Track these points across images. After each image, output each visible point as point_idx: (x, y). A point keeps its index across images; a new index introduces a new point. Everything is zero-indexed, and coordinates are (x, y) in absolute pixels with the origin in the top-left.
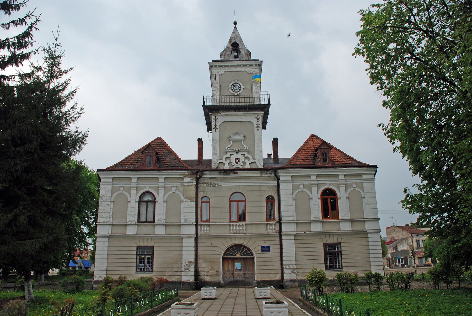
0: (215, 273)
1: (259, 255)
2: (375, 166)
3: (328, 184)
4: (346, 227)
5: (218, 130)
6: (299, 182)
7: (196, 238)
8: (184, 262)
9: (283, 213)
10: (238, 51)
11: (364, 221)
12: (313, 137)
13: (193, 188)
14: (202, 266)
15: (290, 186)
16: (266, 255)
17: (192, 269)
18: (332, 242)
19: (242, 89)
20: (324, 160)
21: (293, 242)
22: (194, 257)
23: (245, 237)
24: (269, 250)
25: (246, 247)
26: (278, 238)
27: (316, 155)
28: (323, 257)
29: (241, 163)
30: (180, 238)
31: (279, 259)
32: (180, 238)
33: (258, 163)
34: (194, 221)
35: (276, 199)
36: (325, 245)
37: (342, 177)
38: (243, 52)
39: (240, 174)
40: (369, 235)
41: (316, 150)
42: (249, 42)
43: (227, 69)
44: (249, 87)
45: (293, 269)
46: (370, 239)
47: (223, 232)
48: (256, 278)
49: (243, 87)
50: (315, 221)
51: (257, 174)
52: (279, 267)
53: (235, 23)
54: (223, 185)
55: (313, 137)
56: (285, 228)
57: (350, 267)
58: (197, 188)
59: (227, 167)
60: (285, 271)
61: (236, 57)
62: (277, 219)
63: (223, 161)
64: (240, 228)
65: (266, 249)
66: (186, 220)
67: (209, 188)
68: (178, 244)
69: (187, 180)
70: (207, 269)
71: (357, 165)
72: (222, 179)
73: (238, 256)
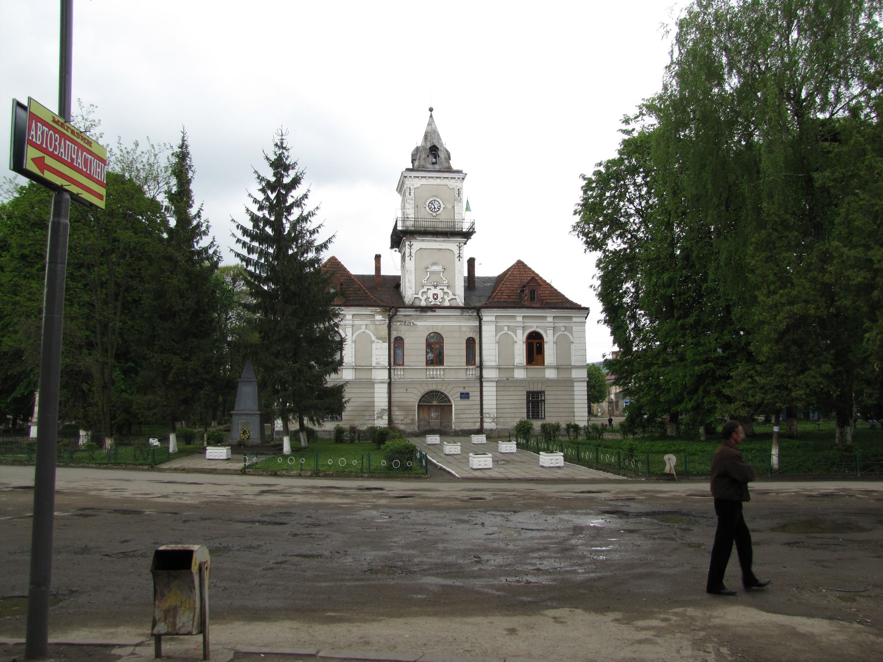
0: (410, 421)
1: (458, 403)
2: (587, 309)
3: (534, 326)
4: (550, 374)
5: (413, 259)
6: (504, 323)
7: (390, 384)
8: (377, 410)
9: (485, 358)
10: (436, 156)
11: (570, 368)
12: (520, 265)
13: (385, 327)
14: (398, 414)
15: (493, 328)
16: (465, 402)
17: (386, 417)
18: (536, 390)
19: (442, 209)
20: (532, 299)
21: (495, 389)
22: (387, 404)
23: (443, 382)
24: (468, 398)
25: (442, 393)
26: (478, 385)
27: (522, 291)
28: (525, 406)
29: (439, 299)
30: (371, 383)
31: (479, 407)
32: (371, 383)
33: (458, 300)
34: (387, 364)
35: (477, 341)
36: (528, 393)
37: (551, 319)
38: (442, 155)
39: (439, 312)
40: (575, 384)
41: (524, 287)
42: (448, 141)
43: (424, 181)
44: (450, 206)
45: (494, 418)
46: (575, 388)
47: (418, 376)
48: (453, 427)
49: (442, 206)
50: (518, 367)
51: (457, 313)
52: (479, 415)
53: (431, 110)
54: (419, 323)
55: (520, 265)
56: (486, 374)
57: (553, 415)
58: (389, 327)
59: (423, 303)
60: (486, 420)
61: (433, 163)
62: (478, 363)
63: (420, 296)
64: (436, 372)
65: (465, 396)
66: (378, 363)
67: (403, 328)
68: (370, 390)
69: (379, 317)
70: (401, 418)
71: (568, 306)
72: (418, 318)
73: (435, 403)
